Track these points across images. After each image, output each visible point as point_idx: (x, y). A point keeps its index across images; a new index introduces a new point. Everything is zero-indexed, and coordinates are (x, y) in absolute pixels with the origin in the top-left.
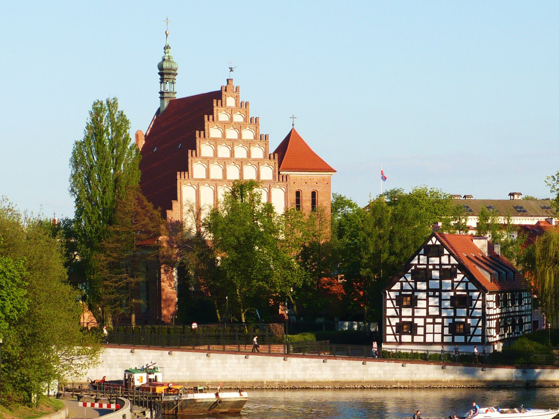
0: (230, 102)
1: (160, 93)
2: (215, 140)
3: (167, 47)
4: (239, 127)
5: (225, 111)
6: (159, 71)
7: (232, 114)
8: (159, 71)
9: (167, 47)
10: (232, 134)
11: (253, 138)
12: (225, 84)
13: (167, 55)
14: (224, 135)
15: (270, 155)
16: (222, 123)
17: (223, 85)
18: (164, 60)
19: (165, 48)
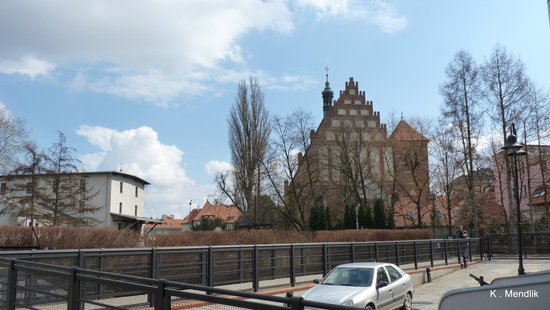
0: (352, 92)
1: (323, 108)
2: (341, 116)
3: (327, 84)
4: (359, 108)
5: (348, 97)
6: (322, 96)
7: (353, 100)
8: (322, 96)
9: (327, 84)
10: (353, 112)
11: (368, 114)
12: (349, 81)
13: (327, 87)
14: (348, 112)
15: (382, 124)
16: (346, 105)
17: (347, 81)
18: (325, 89)
19: (326, 83)
